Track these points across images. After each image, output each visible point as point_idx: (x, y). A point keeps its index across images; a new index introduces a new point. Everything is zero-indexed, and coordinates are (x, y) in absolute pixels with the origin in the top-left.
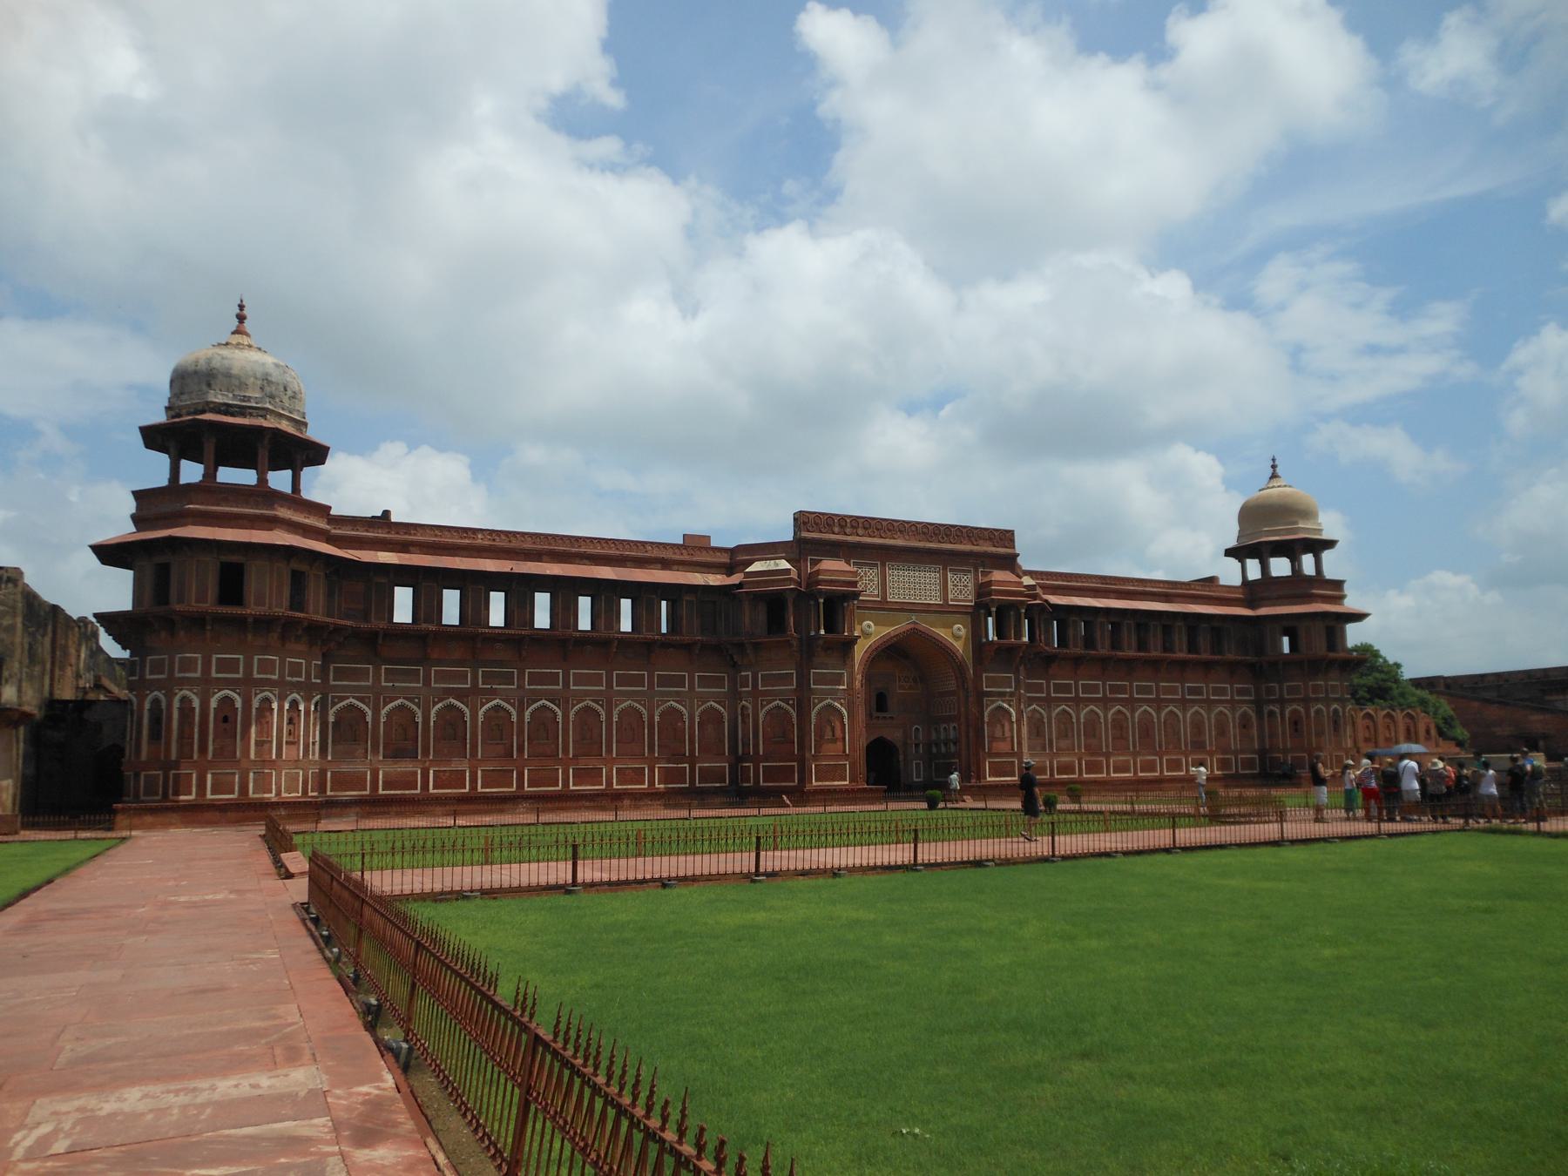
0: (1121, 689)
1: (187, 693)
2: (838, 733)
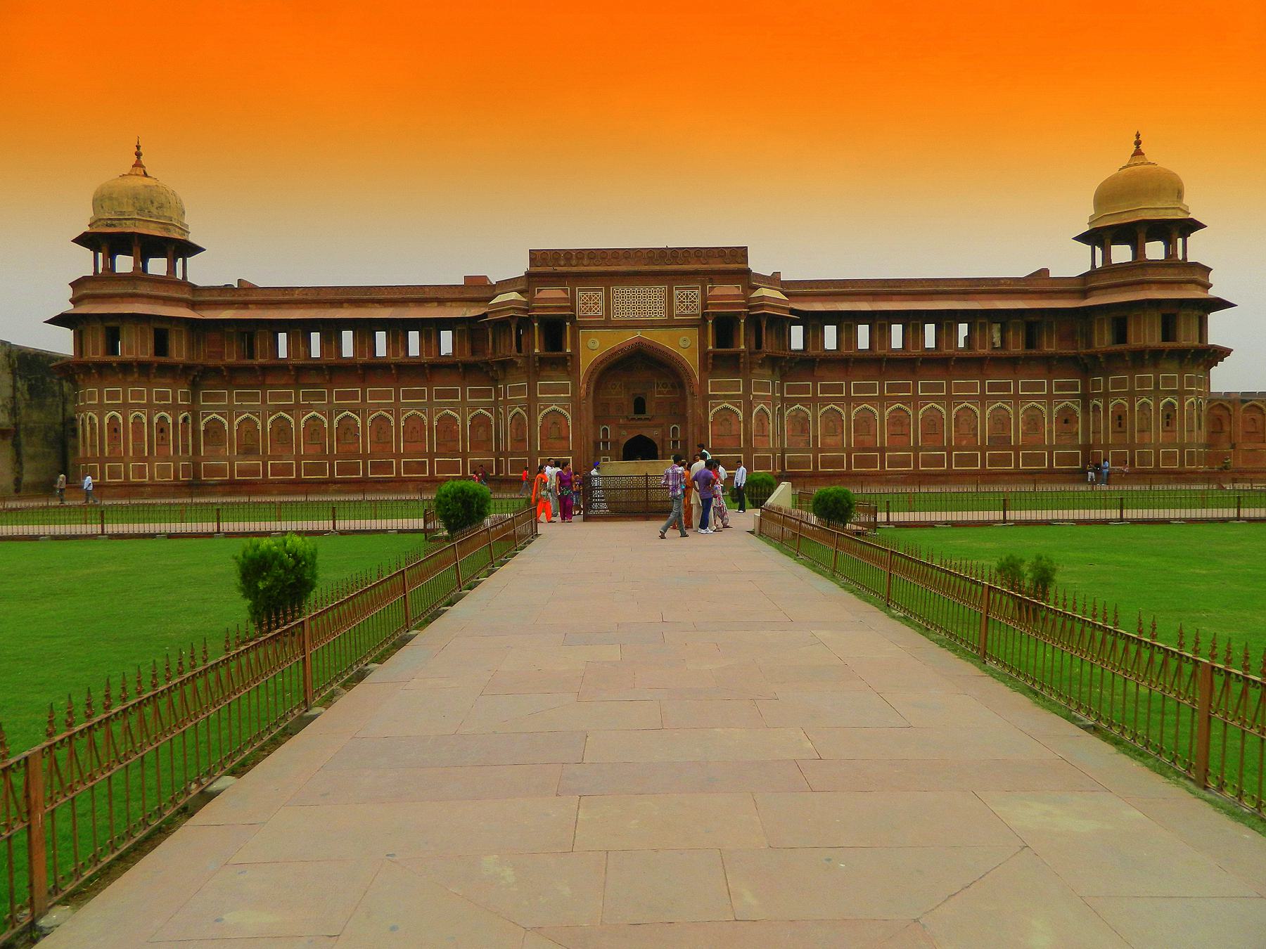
0: (906, 388)
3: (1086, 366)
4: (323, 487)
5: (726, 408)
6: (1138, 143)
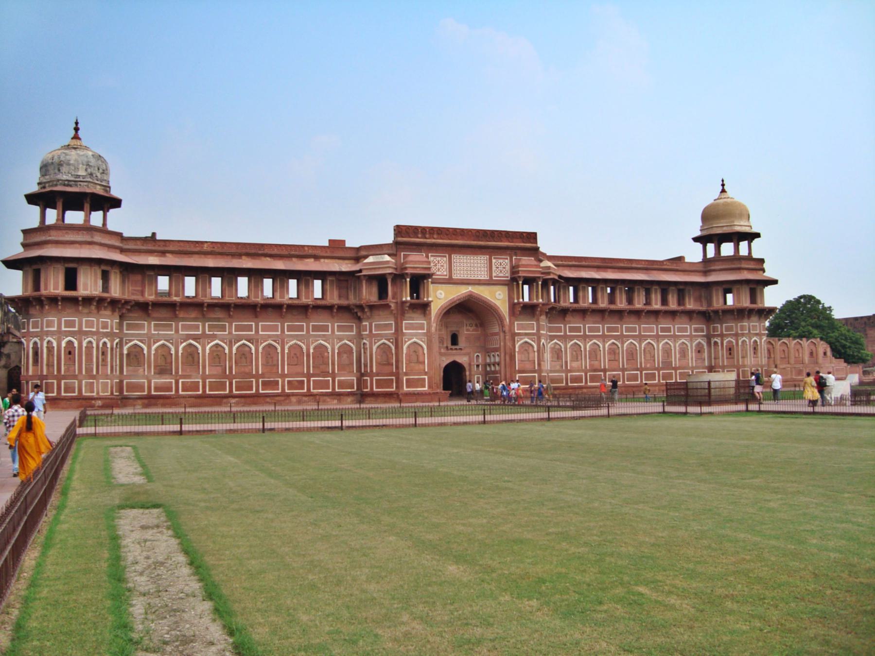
1: (49, 338)
2: (421, 359)
3: (708, 317)
4: (225, 400)
5: (526, 342)
6: (723, 185)
